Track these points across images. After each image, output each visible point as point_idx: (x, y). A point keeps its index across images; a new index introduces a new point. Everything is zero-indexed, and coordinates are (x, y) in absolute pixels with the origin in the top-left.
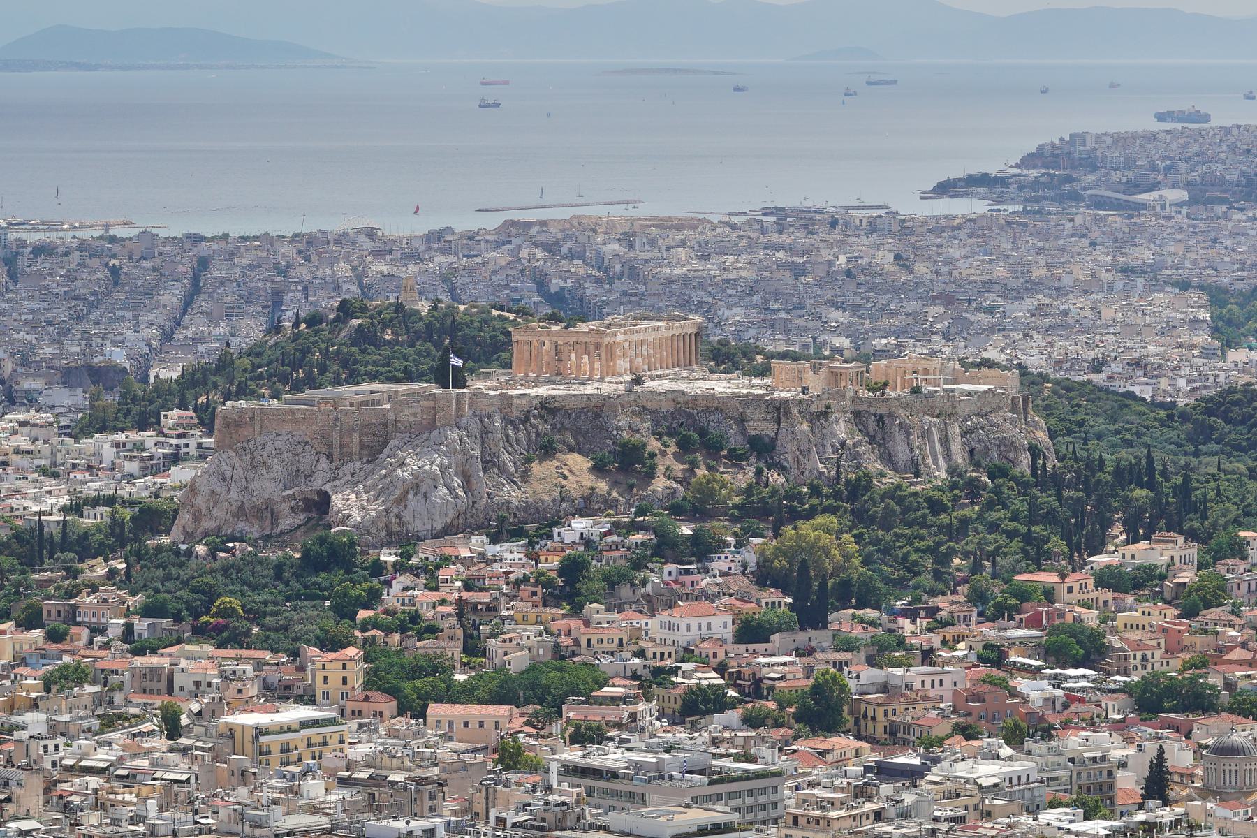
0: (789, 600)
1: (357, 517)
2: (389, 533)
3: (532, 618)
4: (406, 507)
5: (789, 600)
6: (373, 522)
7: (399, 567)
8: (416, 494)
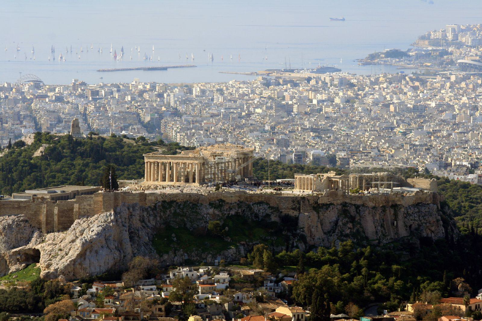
4: (85, 259)
8: (91, 251)
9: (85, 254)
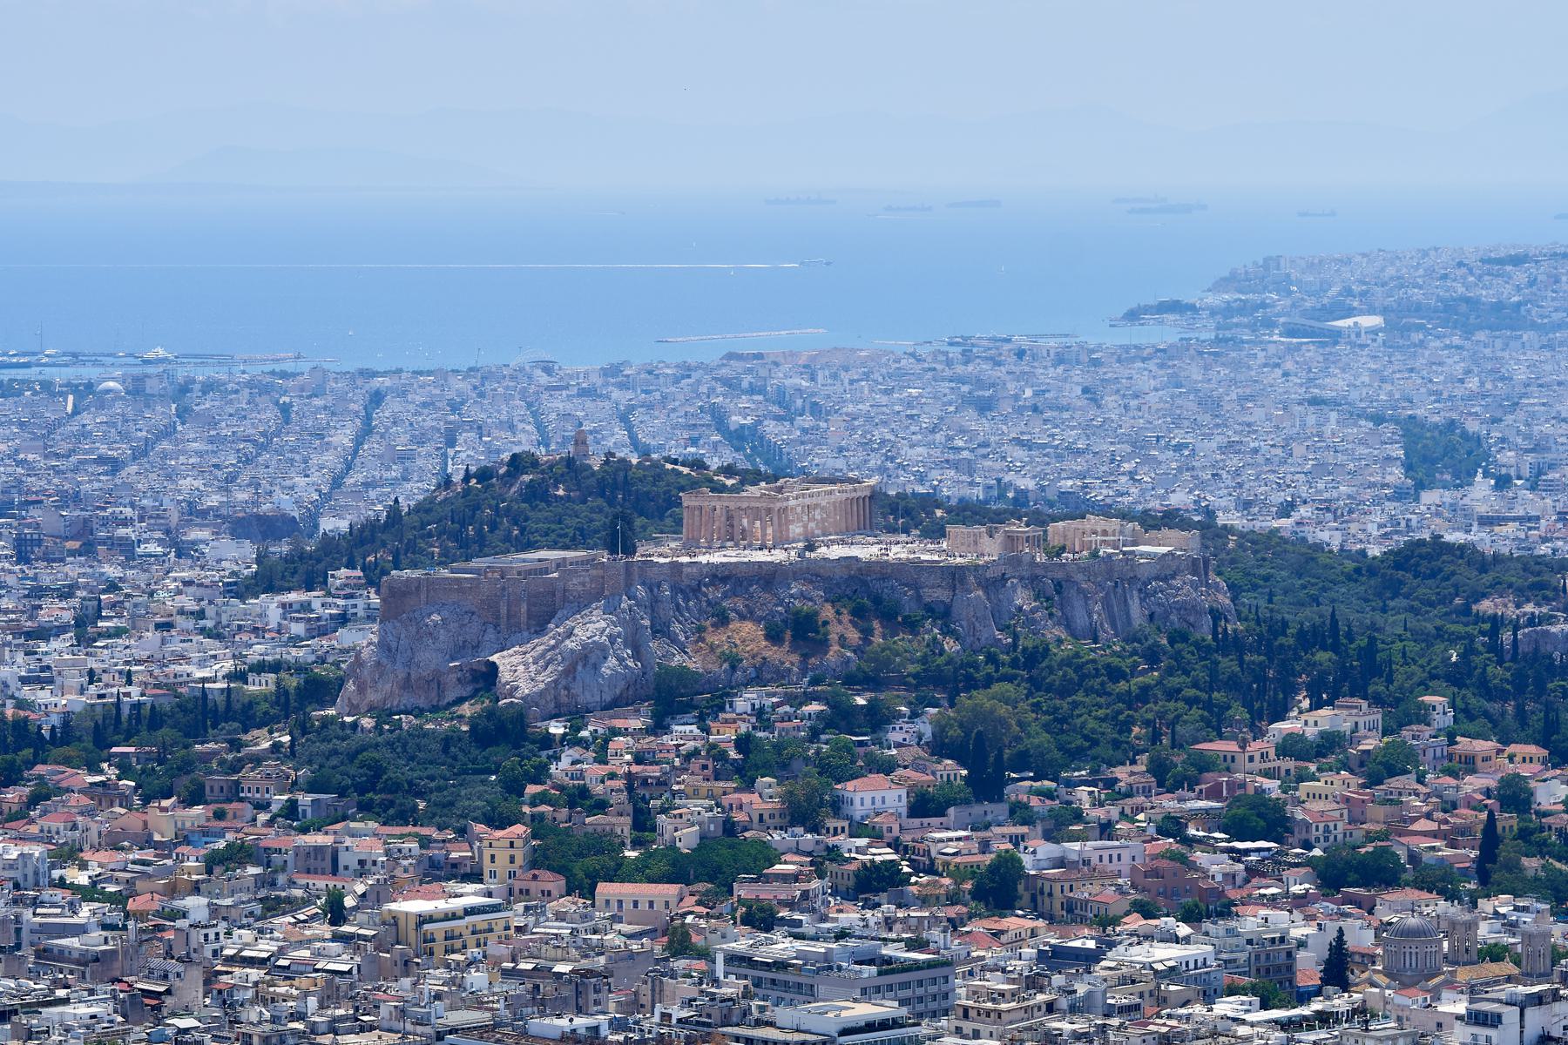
0: (964, 772)
1: (525, 689)
2: (558, 705)
3: (703, 792)
5: (964, 772)
6: (541, 693)
7: (571, 740)
9: (575, 669)
